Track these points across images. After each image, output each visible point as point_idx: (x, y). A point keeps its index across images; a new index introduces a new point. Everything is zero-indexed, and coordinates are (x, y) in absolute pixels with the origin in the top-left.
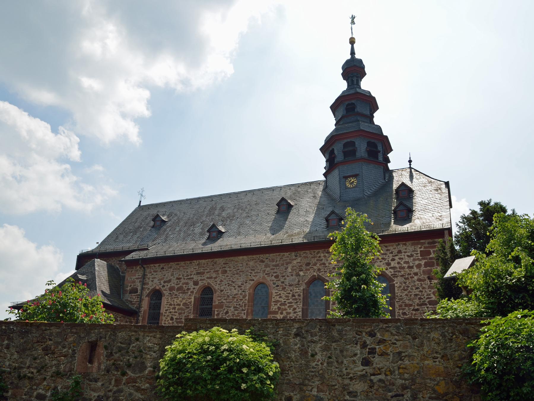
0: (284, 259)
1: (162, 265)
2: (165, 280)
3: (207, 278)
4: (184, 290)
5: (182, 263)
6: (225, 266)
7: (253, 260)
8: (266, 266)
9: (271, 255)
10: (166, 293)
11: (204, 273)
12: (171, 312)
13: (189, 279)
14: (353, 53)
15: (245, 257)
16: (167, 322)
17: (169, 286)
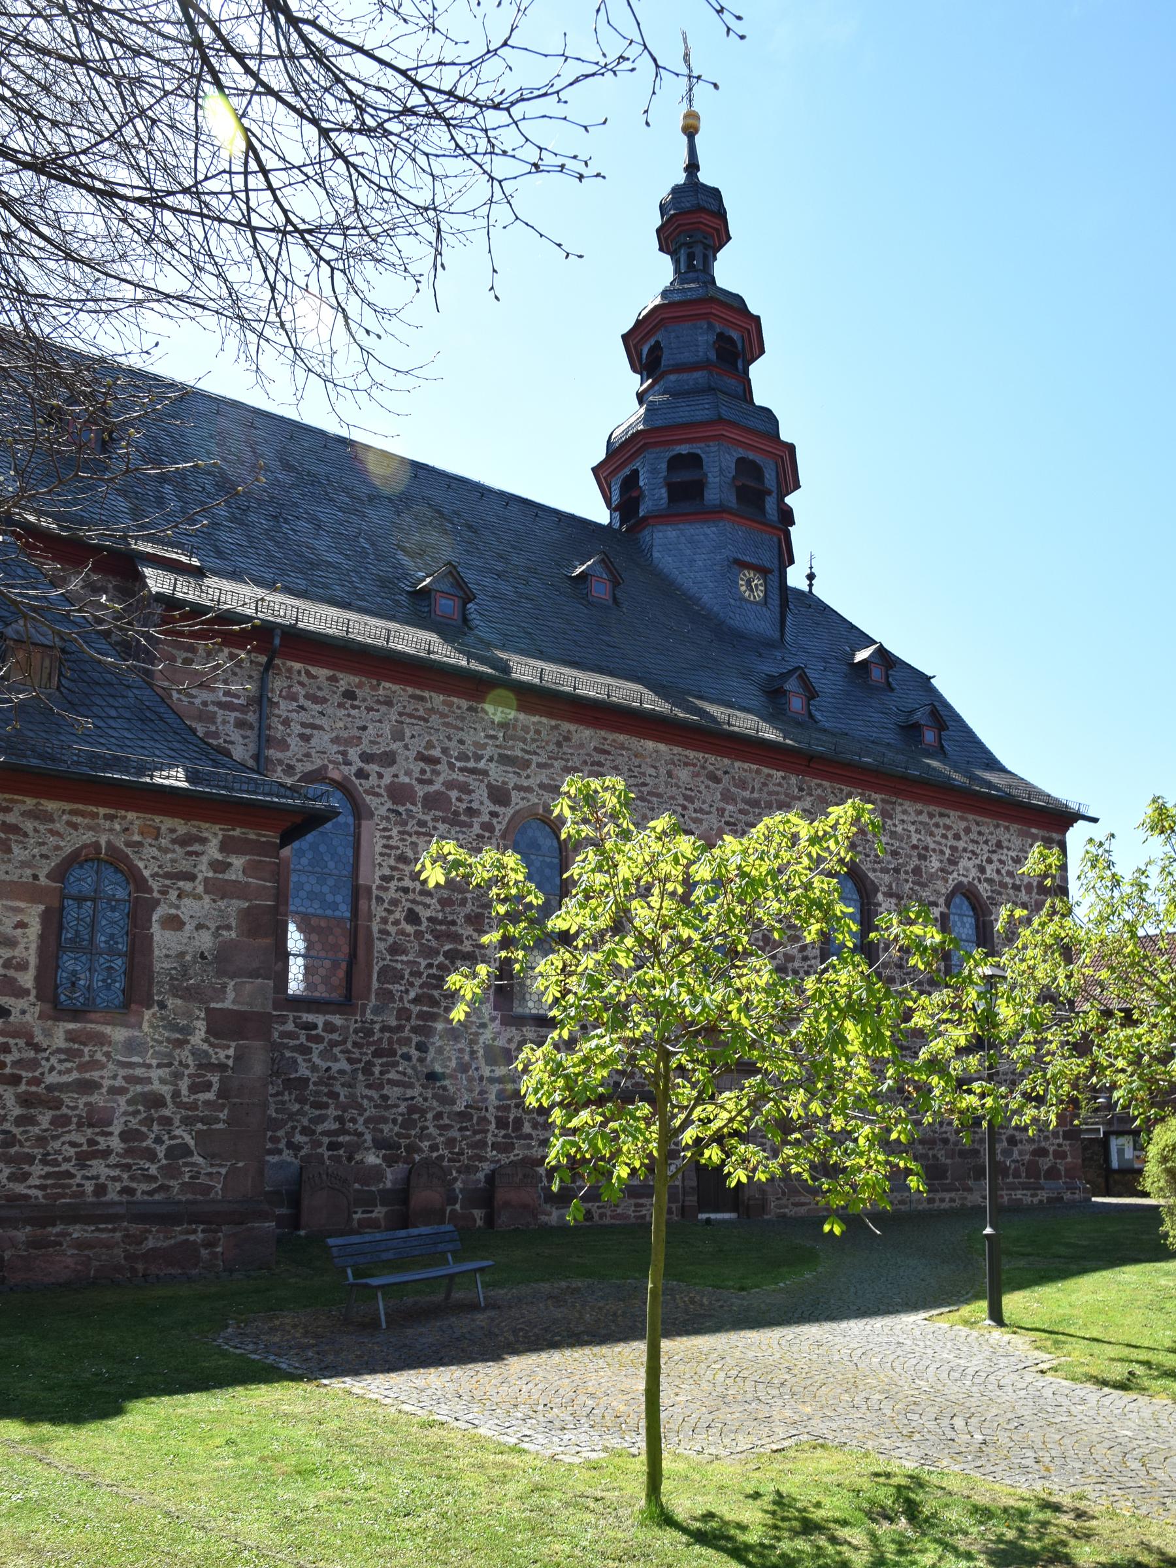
0: (771, 788)
1: (346, 680)
2: (365, 746)
3: (542, 786)
4: (456, 813)
5: (438, 699)
6: (602, 758)
7: (686, 764)
8: (727, 797)
9: (737, 764)
10: (380, 806)
11: (526, 764)
12: (406, 890)
13: (473, 771)
14: (692, 167)
15: (662, 747)
16: (392, 929)
17: (387, 780)
